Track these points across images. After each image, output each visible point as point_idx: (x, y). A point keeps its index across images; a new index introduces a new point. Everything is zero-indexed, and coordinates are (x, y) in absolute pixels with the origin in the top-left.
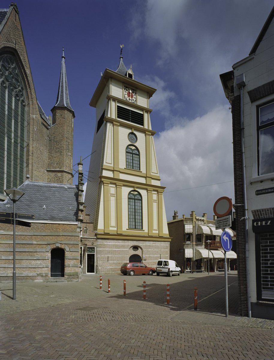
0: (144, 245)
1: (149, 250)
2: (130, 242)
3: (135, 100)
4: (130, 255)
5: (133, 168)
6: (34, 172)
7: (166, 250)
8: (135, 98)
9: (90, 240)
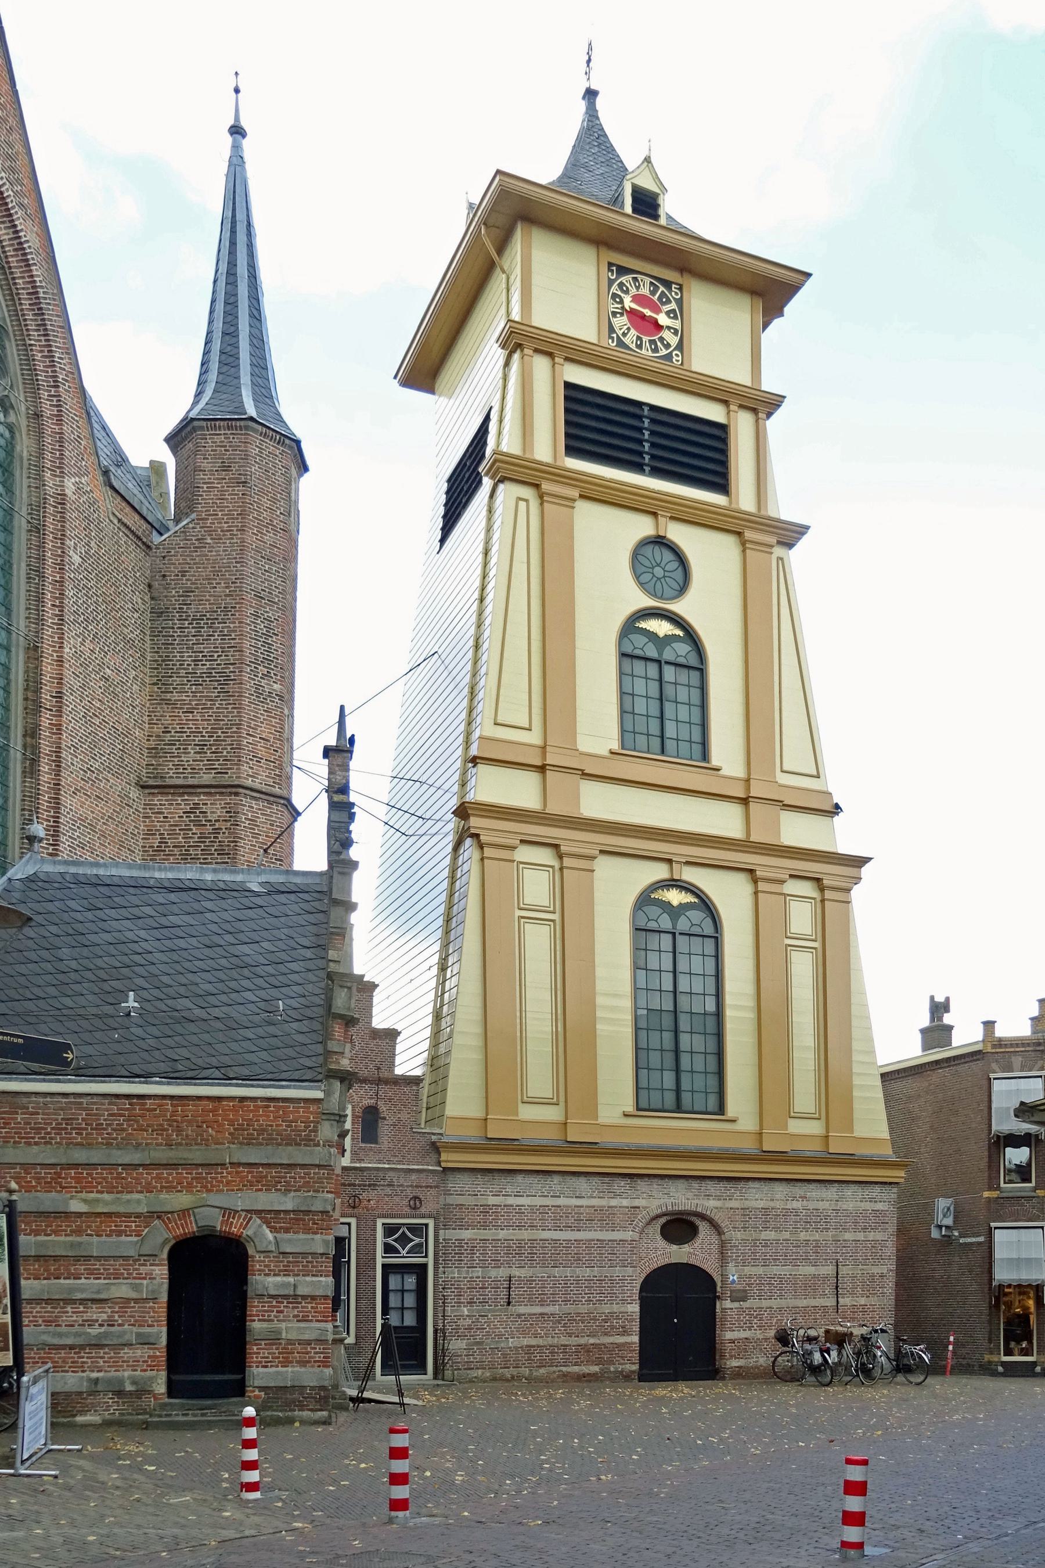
0: (733, 1204)
1: (765, 1235)
2: (642, 1185)
3: (673, 340)
4: (648, 1271)
5: (663, 752)
6: (68, 801)
7: (871, 1236)
8: (676, 332)
9: (402, 1181)
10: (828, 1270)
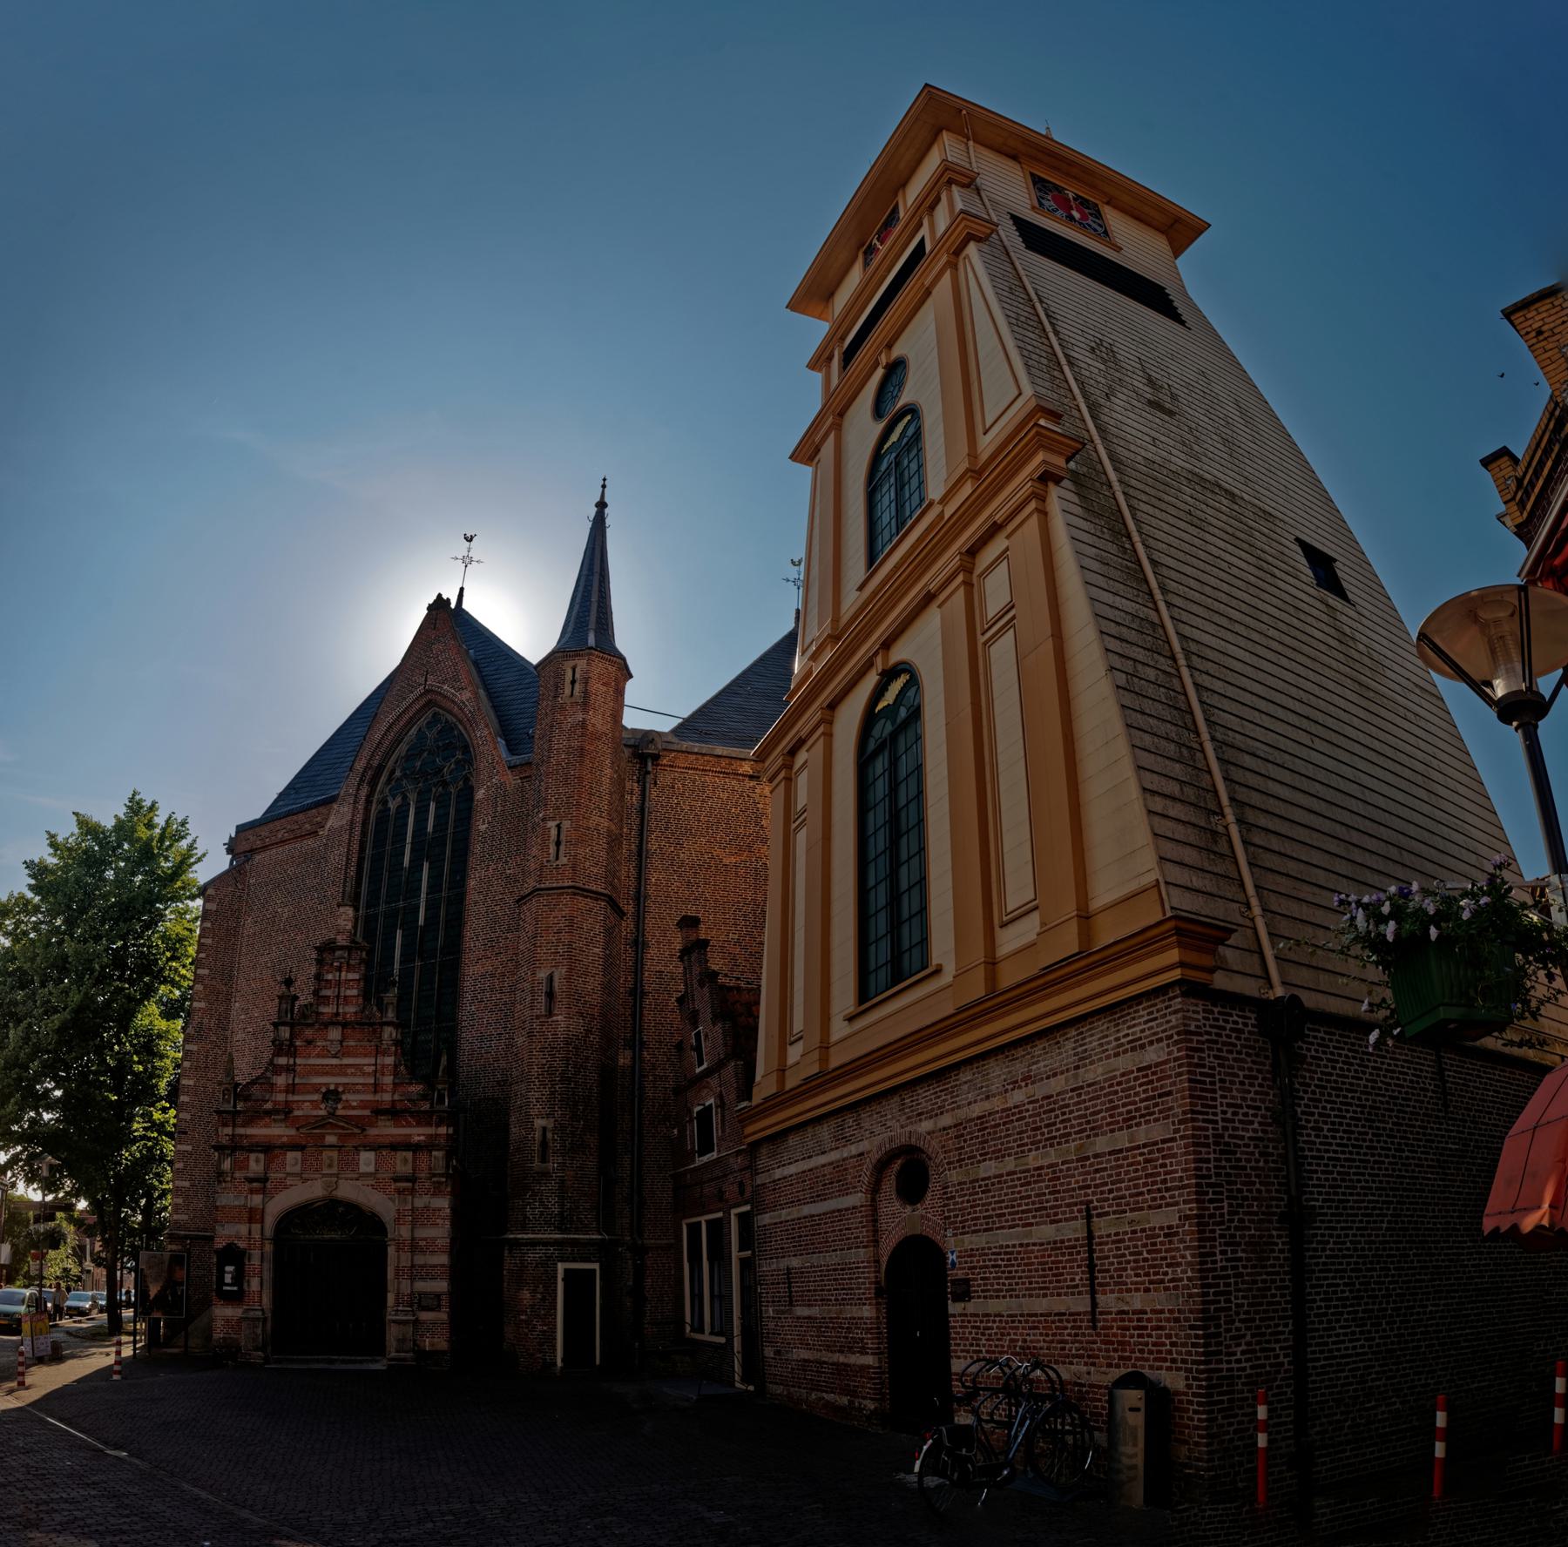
0: (946, 1120)
7: (1142, 1134)
10: (1075, 1230)
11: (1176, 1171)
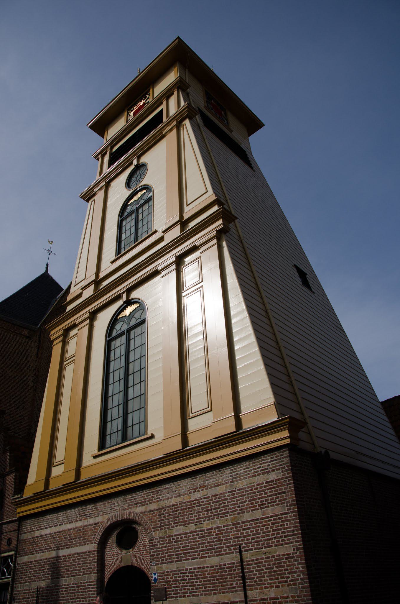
0: (153, 506)
7: (269, 511)
10: (233, 559)
11: (290, 528)
